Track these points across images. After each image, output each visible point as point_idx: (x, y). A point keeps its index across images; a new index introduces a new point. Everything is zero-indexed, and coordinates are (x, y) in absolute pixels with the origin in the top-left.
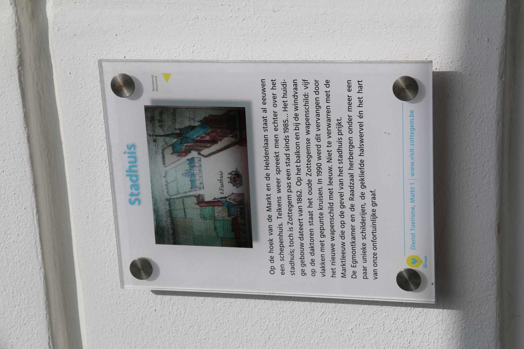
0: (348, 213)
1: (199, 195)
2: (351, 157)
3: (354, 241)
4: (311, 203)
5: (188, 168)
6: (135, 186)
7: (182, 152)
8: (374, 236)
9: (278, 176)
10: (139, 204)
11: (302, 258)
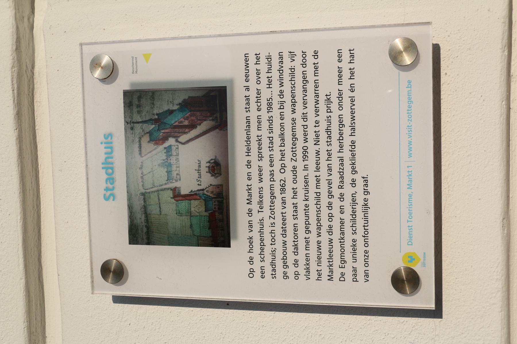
0: (336, 203)
1: (176, 187)
2: (341, 138)
3: (342, 237)
4: (295, 193)
5: (165, 158)
6: (111, 179)
7: (159, 140)
8: (366, 230)
9: (261, 163)
10: (113, 200)
11: (285, 258)
